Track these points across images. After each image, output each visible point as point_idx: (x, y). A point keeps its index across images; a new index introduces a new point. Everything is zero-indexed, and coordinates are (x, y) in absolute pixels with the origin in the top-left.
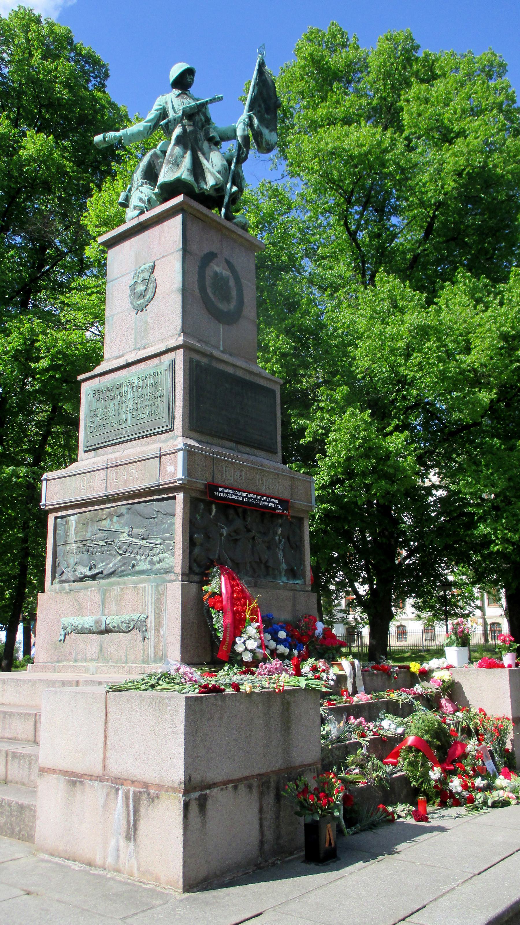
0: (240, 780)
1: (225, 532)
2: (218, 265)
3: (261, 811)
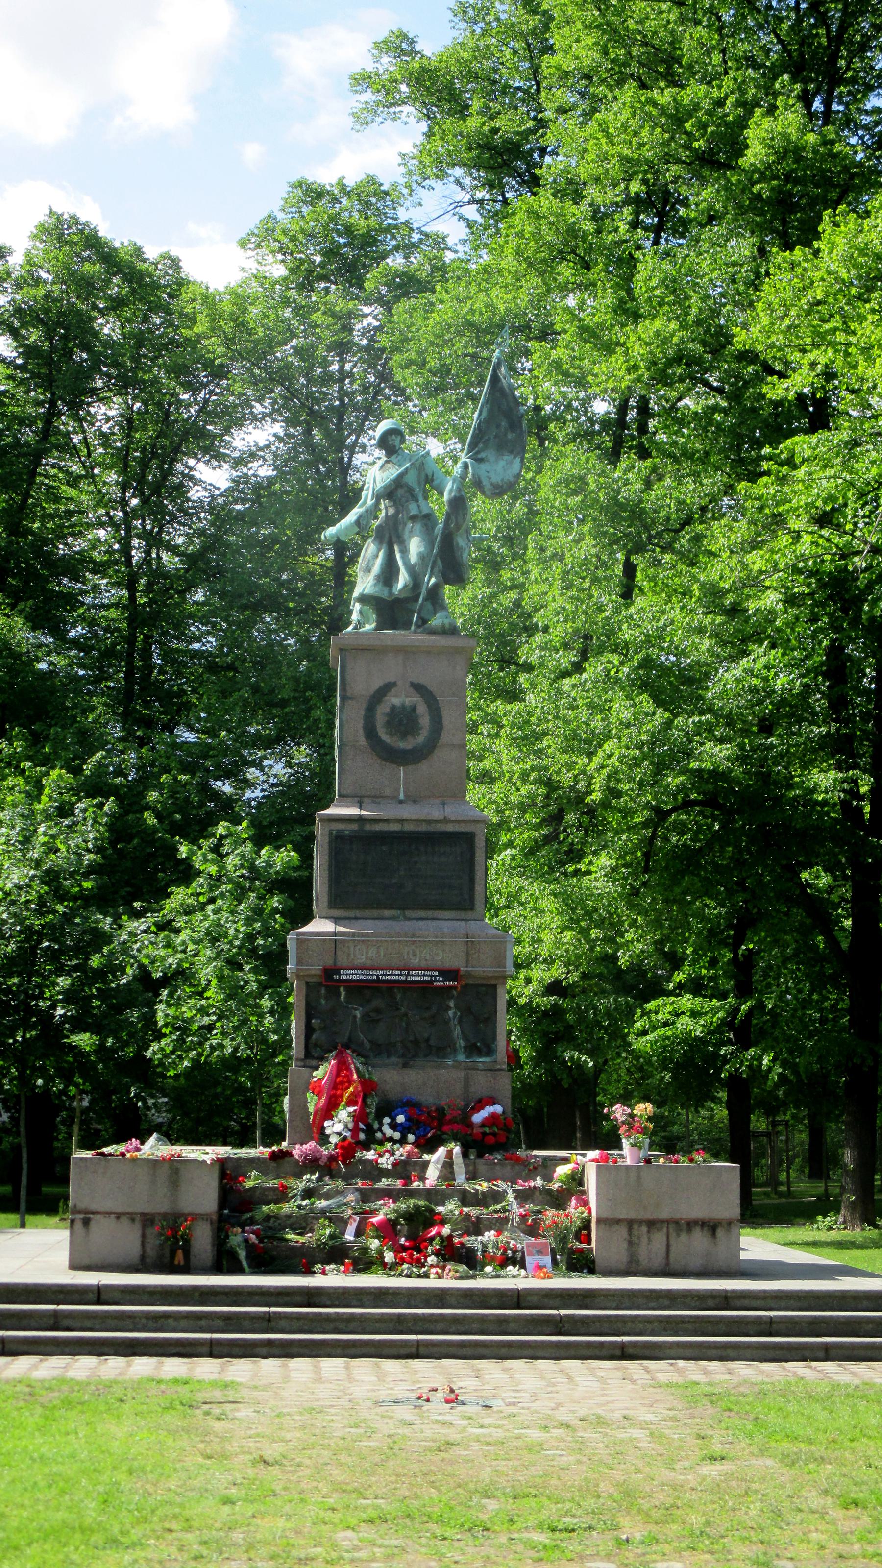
0: (124, 1214)
1: (358, 1014)
2: (396, 696)
3: (144, 1236)
